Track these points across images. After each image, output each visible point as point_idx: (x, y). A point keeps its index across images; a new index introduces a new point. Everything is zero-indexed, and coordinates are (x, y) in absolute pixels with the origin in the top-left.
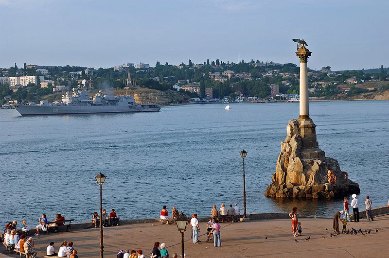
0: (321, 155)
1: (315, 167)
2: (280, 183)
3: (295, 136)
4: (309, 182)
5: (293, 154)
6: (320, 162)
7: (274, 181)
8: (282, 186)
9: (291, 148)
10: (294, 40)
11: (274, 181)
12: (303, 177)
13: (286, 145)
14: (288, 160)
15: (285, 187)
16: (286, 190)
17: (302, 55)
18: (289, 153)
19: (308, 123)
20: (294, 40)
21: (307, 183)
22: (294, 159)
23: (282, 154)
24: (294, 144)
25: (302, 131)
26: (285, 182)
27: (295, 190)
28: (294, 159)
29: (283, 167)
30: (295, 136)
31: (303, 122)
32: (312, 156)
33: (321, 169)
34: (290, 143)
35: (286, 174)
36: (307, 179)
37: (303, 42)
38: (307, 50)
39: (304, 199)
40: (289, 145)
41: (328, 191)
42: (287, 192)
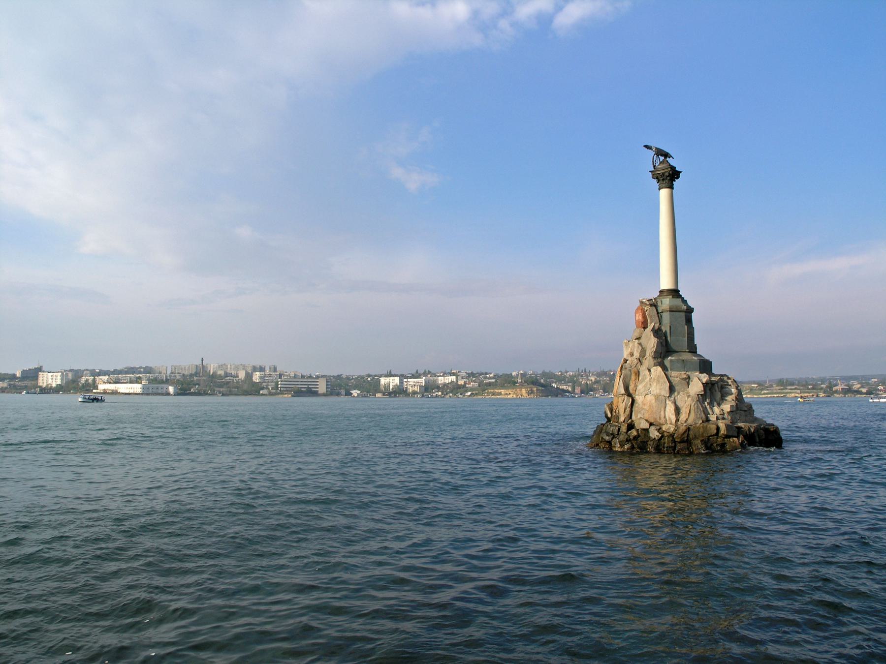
0: (705, 366)
1: (696, 387)
2: (622, 419)
3: (650, 327)
4: (683, 417)
5: (649, 360)
6: (705, 378)
7: (609, 415)
8: (624, 428)
9: (643, 352)
10: (646, 147)
11: (609, 415)
12: (670, 408)
13: (634, 345)
14: (638, 374)
15: (631, 426)
16: (634, 433)
17: (663, 174)
18: (640, 361)
19: (678, 302)
20: (647, 147)
21: (677, 420)
22: (650, 371)
23: (626, 361)
24: (651, 343)
25: (666, 317)
26: (631, 418)
27: (654, 434)
28: (650, 371)
29: (627, 388)
30: (650, 327)
31: (666, 303)
32: (684, 365)
33: (708, 391)
34: (642, 341)
35: (633, 401)
36: (677, 411)
37: (667, 155)
38: (673, 168)
39: (673, 451)
40: (640, 344)
41: (727, 437)
42: (635, 438)
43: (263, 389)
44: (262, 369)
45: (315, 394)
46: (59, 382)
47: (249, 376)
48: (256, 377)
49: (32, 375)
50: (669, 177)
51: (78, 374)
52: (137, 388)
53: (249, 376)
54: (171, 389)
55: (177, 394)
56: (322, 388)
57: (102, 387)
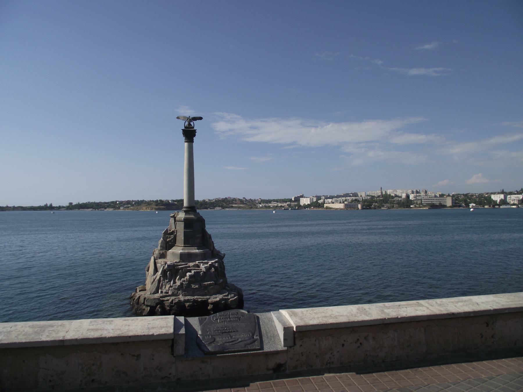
10: (178, 118)
20: (178, 118)
43: (412, 205)
44: (417, 192)
45: (445, 206)
46: (309, 203)
47: (408, 196)
48: (412, 197)
49: (297, 199)
50: (189, 134)
51: (319, 198)
52: (342, 206)
53: (408, 196)
54: (360, 206)
55: (363, 208)
56: (449, 202)
57: (325, 205)
